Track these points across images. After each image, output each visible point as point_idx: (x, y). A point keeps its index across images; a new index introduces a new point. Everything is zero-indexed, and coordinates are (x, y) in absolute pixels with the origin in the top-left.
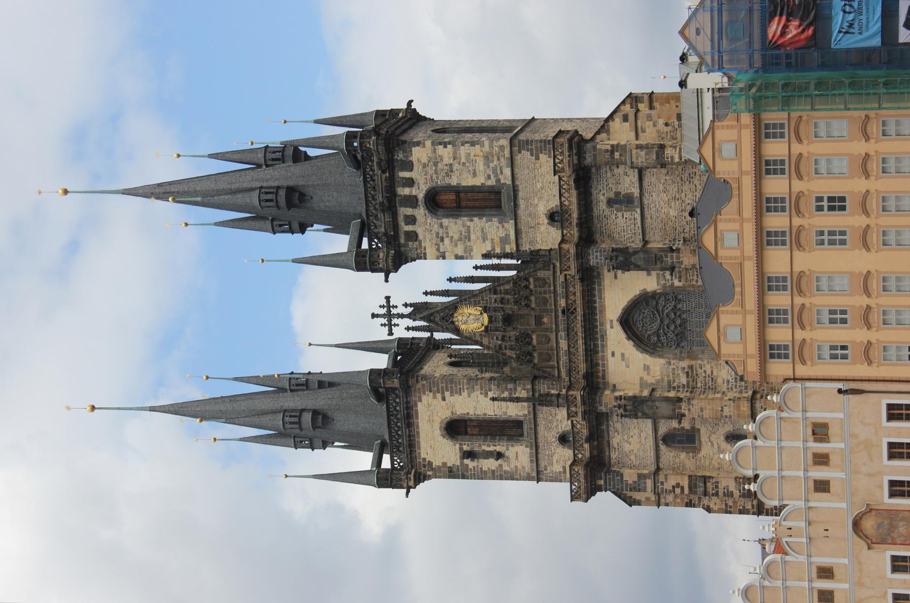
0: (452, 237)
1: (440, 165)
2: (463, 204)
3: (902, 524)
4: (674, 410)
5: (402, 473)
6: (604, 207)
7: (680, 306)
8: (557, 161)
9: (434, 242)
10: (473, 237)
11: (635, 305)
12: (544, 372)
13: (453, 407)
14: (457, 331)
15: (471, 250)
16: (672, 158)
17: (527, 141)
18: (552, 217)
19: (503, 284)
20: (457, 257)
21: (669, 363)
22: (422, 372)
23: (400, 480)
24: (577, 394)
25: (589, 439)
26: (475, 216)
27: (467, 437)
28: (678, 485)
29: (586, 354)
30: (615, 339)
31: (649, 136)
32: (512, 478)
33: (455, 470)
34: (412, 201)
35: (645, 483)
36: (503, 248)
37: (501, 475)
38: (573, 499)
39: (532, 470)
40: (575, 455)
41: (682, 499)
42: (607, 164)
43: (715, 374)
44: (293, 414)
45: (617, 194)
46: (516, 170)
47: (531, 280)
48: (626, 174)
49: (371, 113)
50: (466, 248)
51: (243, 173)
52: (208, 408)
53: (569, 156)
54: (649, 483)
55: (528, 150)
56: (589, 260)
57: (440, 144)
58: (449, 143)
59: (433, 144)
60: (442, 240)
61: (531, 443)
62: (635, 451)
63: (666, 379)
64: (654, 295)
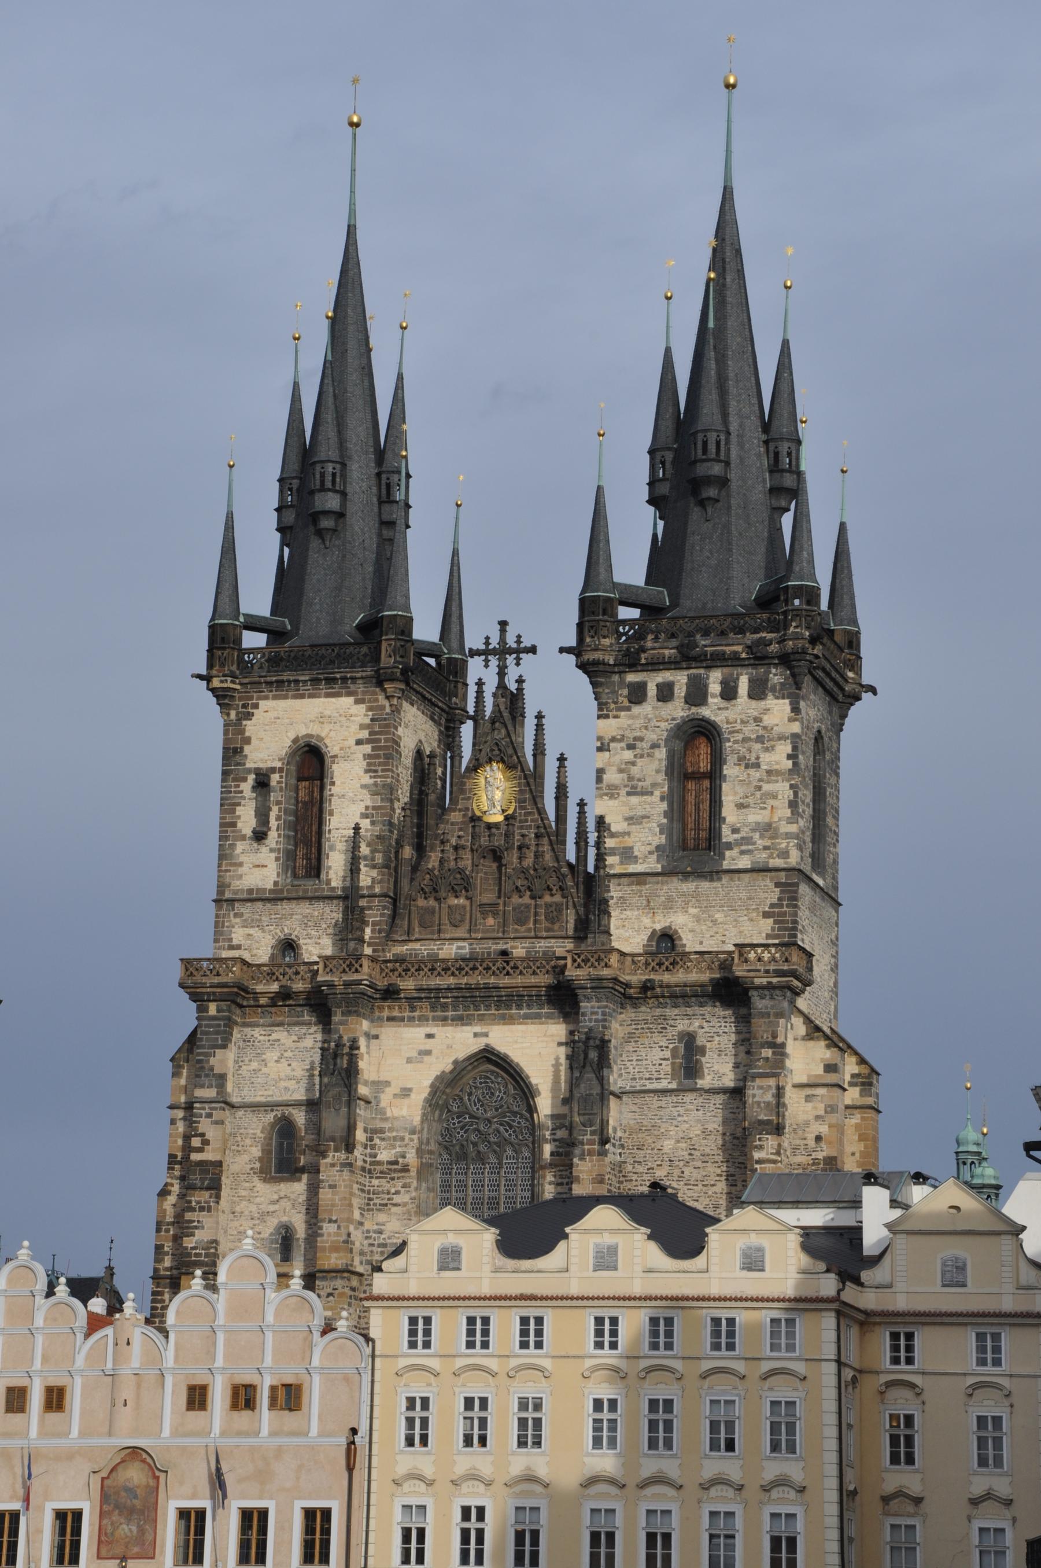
0: (633, 764)
1: (758, 746)
2: (691, 785)
3: (134, 1528)
4: (333, 1139)
5: (234, 668)
6: (680, 1028)
7: (510, 1152)
8: (759, 950)
9: (628, 733)
10: (634, 800)
13: (346, 758)
14: (475, 766)
15: (612, 796)
16: (761, 1147)
18: (666, 940)
19: (553, 850)
20: (600, 772)
21: (413, 1132)
22: (406, 705)
23: (222, 665)
26: (671, 805)
27: (293, 781)
28: (206, 1142)
29: (430, 990)
30: (458, 1041)
31: (798, 1108)
32: (222, 857)
33: (238, 758)
34: (697, 695)
36: (613, 852)
37: (227, 838)
39: (236, 892)
43: (394, 1209)
45: (702, 1051)
46: (746, 877)
49: (855, 622)
50: (616, 787)
51: (755, 401)
52: (351, 329)
53: (767, 971)
55: (779, 899)
56: (588, 999)
57: (795, 748)
58: (795, 764)
59: (795, 736)
60: (631, 747)
61: (282, 891)
62: (264, 1070)
63: (386, 1125)
64: (532, 1109)
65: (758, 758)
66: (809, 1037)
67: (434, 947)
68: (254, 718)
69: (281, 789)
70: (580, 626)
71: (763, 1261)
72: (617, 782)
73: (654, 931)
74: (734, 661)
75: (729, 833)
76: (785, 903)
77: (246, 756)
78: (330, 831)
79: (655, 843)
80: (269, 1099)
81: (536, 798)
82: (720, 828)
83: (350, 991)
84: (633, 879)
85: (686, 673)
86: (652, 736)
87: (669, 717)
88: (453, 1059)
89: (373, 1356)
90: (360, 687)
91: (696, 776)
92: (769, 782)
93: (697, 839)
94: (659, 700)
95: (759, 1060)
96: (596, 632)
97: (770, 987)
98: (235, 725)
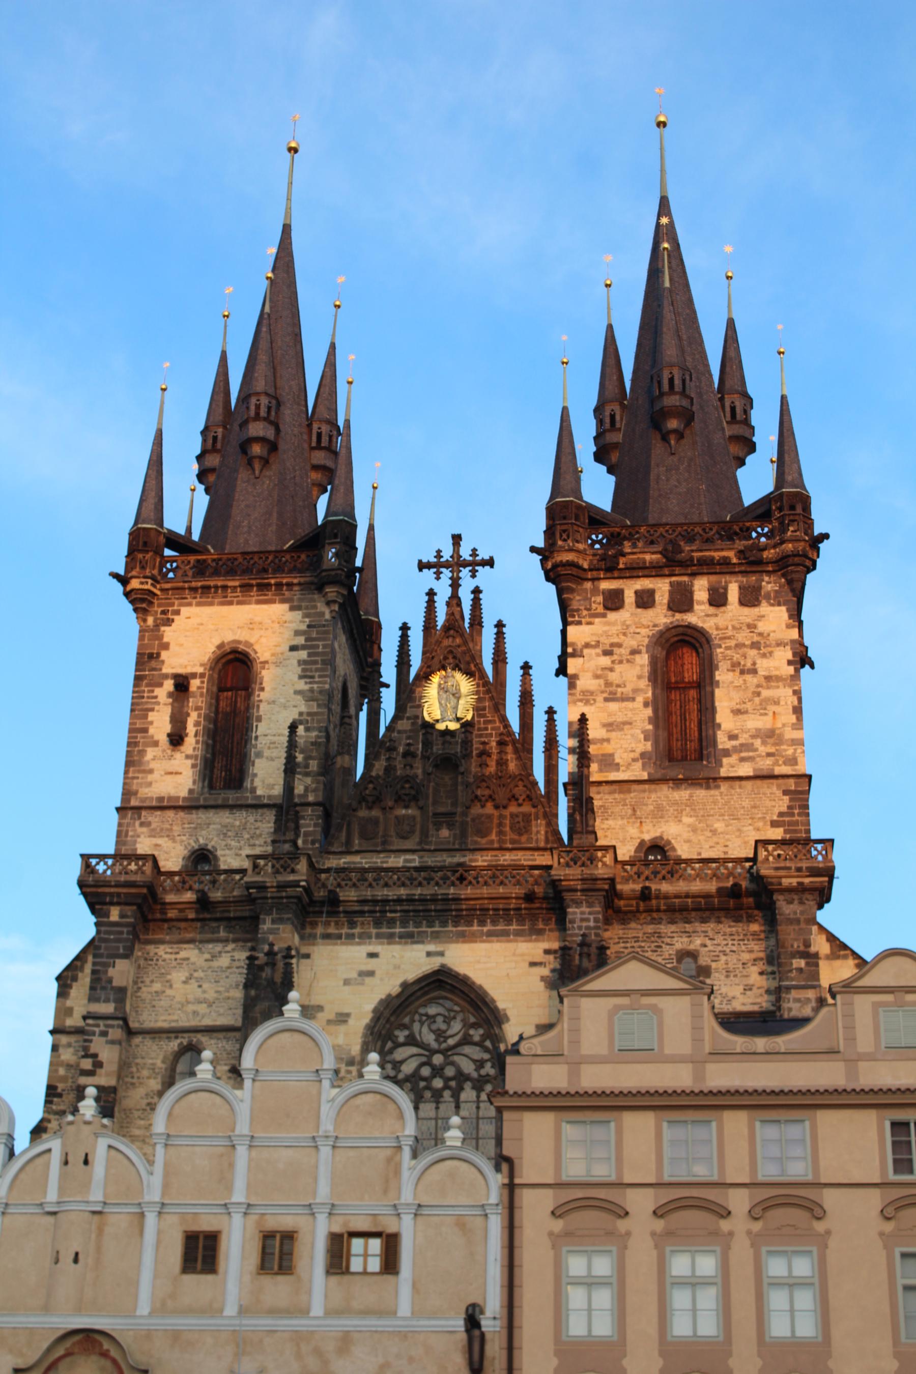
0: (611, 670)
1: (753, 653)
2: (675, 695)
5: (155, 572)
6: (678, 946)
9: (602, 640)
10: (613, 706)
14: (424, 676)
15: (587, 702)
19: (519, 758)
23: (143, 568)
26: (655, 711)
27: (215, 689)
29: (375, 902)
30: (405, 961)
32: (129, 763)
33: (153, 664)
34: (681, 601)
35: (107, 1001)
37: (136, 744)
38: (85, 857)
40: (171, 874)
41: (64, 1079)
44: (273, 413)
46: (748, 784)
48: (748, 988)
50: (592, 693)
53: (799, 869)
54: (108, 1008)
55: (789, 807)
56: (578, 904)
60: (607, 653)
61: (198, 799)
62: (169, 992)
65: (754, 664)
67: (378, 860)
68: (173, 625)
69: (202, 695)
70: (549, 533)
72: (592, 688)
73: (642, 842)
74: (724, 567)
75: (726, 739)
76: (796, 811)
77: (163, 662)
78: (256, 737)
80: (173, 1024)
81: (499, 705)
82: (715, 735)
83: (284, 894)
84: (614, 787)
85: (667, 580)
86: (630, 643)
87: (651, 624)
88: (400, 981)
89: (511, 1188)
90: (296, 593)
92: (768, 688)
93: (684, 749)
95: (791, 971)
96: (566, 534)
97: (801, 889)
98: (152, 630)
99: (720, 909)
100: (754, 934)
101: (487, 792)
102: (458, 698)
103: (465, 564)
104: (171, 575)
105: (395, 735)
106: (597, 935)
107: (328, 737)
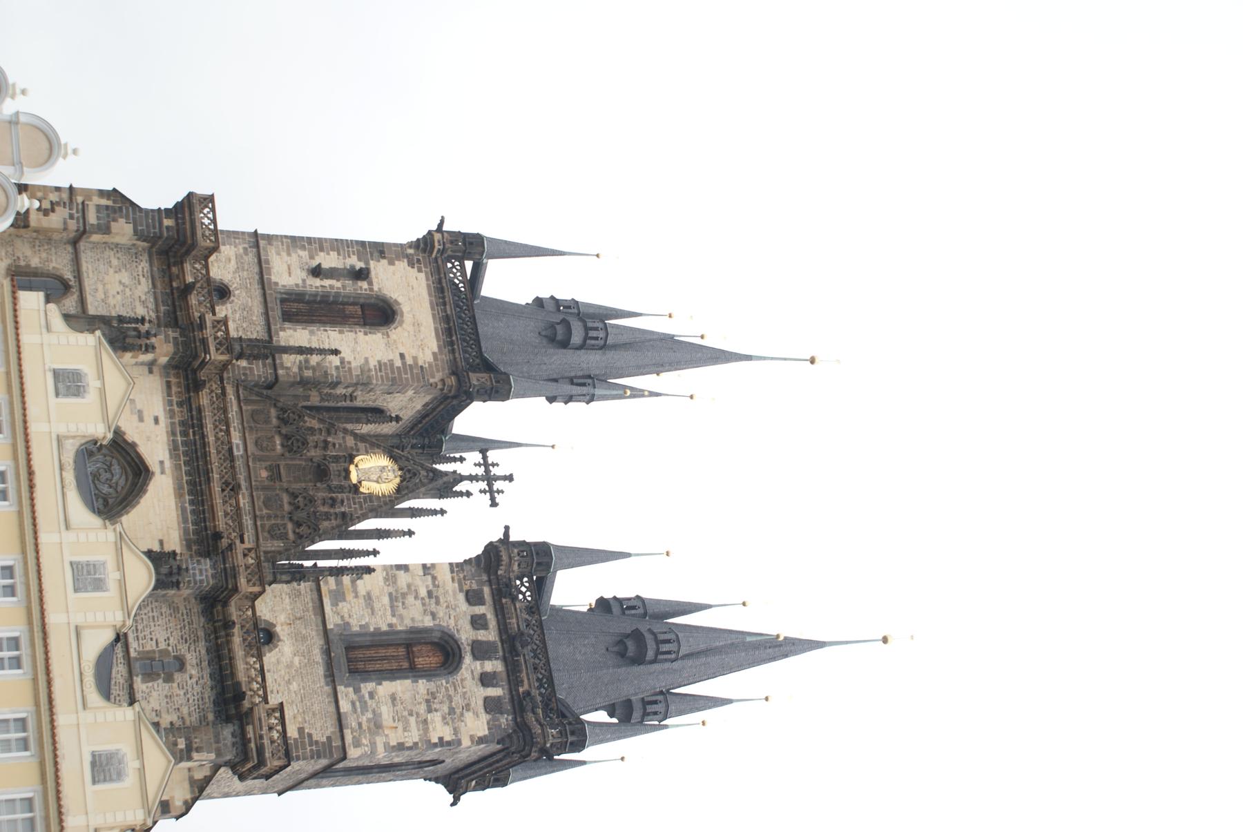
0: (416, 598)
1: (446, 710)
5: (449, 253)
6: (188, 656)
8: (279, 728)
9: (441, 590)
10: (386, 600)
11: (124, 499)
12: (258, 394)
15: (386, 579)
17: (319, 757)
18: (266, 636)
19: (333, 528)
20: (405, 568)
22: (428, 398)
24: (216, 356)
25: (187, 289)
26: (386, 633)
27: (362, 301)
29: (200, 419)
30: (155, 446)
32: (293, 239)
33: (376, 254)
34: (481, 650)
35: (98, 218)
36: (339, 583)
38: (210, 199)
42: (195, 729)
44: (593, 342)
45: (169, 679)
46: (332, 709)
47: (291, 536)
48: (158, 713)
50: (395, 583)
53: (261, 737)
54: (92, 218)
55: (317, 742)
56: (214, 567)
57: (449, 743)
58: (435, 745)
59: (459, 742)
60: (430, 593)
62: (111, 271)
65: (436, 710)
66: (192, 782)
67: (235, 424)
70: (523, 543)
71: (105, 780)
72: (399, 583)
79: (351, 621)
82: (371, 680)
91: (410, 656)
93: (357, 660)
94: (472, 617)
97: (245, 741)
99: (223, 688)
100: (205, 717)
101: (301, 505)
102: (377, 482)
103: (490, 485)
104: (449, 265)
105: (341, 435)
106: (189, 582)
107: (335, 385)
